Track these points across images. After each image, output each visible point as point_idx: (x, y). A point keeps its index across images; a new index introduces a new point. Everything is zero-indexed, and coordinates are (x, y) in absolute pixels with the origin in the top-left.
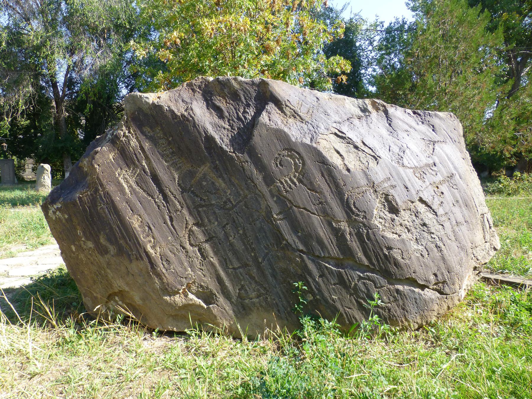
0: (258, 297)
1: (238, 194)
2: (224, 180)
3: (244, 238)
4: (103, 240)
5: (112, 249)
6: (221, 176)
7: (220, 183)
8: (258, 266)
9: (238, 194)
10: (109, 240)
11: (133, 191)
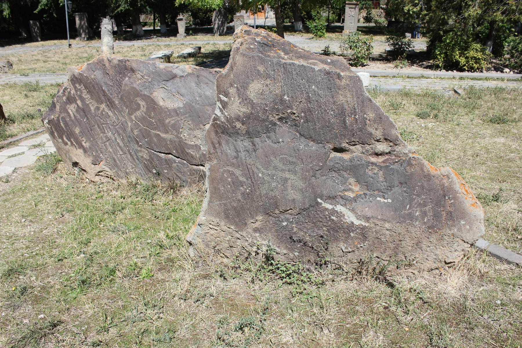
0: (132, 168)
3: (123, 140)
4: (65, 139)
5: (69, 143)
6: (110, 110)
7: (110, 113)
8: (130, 154)
10: (67, 139)
11: (74, 115)
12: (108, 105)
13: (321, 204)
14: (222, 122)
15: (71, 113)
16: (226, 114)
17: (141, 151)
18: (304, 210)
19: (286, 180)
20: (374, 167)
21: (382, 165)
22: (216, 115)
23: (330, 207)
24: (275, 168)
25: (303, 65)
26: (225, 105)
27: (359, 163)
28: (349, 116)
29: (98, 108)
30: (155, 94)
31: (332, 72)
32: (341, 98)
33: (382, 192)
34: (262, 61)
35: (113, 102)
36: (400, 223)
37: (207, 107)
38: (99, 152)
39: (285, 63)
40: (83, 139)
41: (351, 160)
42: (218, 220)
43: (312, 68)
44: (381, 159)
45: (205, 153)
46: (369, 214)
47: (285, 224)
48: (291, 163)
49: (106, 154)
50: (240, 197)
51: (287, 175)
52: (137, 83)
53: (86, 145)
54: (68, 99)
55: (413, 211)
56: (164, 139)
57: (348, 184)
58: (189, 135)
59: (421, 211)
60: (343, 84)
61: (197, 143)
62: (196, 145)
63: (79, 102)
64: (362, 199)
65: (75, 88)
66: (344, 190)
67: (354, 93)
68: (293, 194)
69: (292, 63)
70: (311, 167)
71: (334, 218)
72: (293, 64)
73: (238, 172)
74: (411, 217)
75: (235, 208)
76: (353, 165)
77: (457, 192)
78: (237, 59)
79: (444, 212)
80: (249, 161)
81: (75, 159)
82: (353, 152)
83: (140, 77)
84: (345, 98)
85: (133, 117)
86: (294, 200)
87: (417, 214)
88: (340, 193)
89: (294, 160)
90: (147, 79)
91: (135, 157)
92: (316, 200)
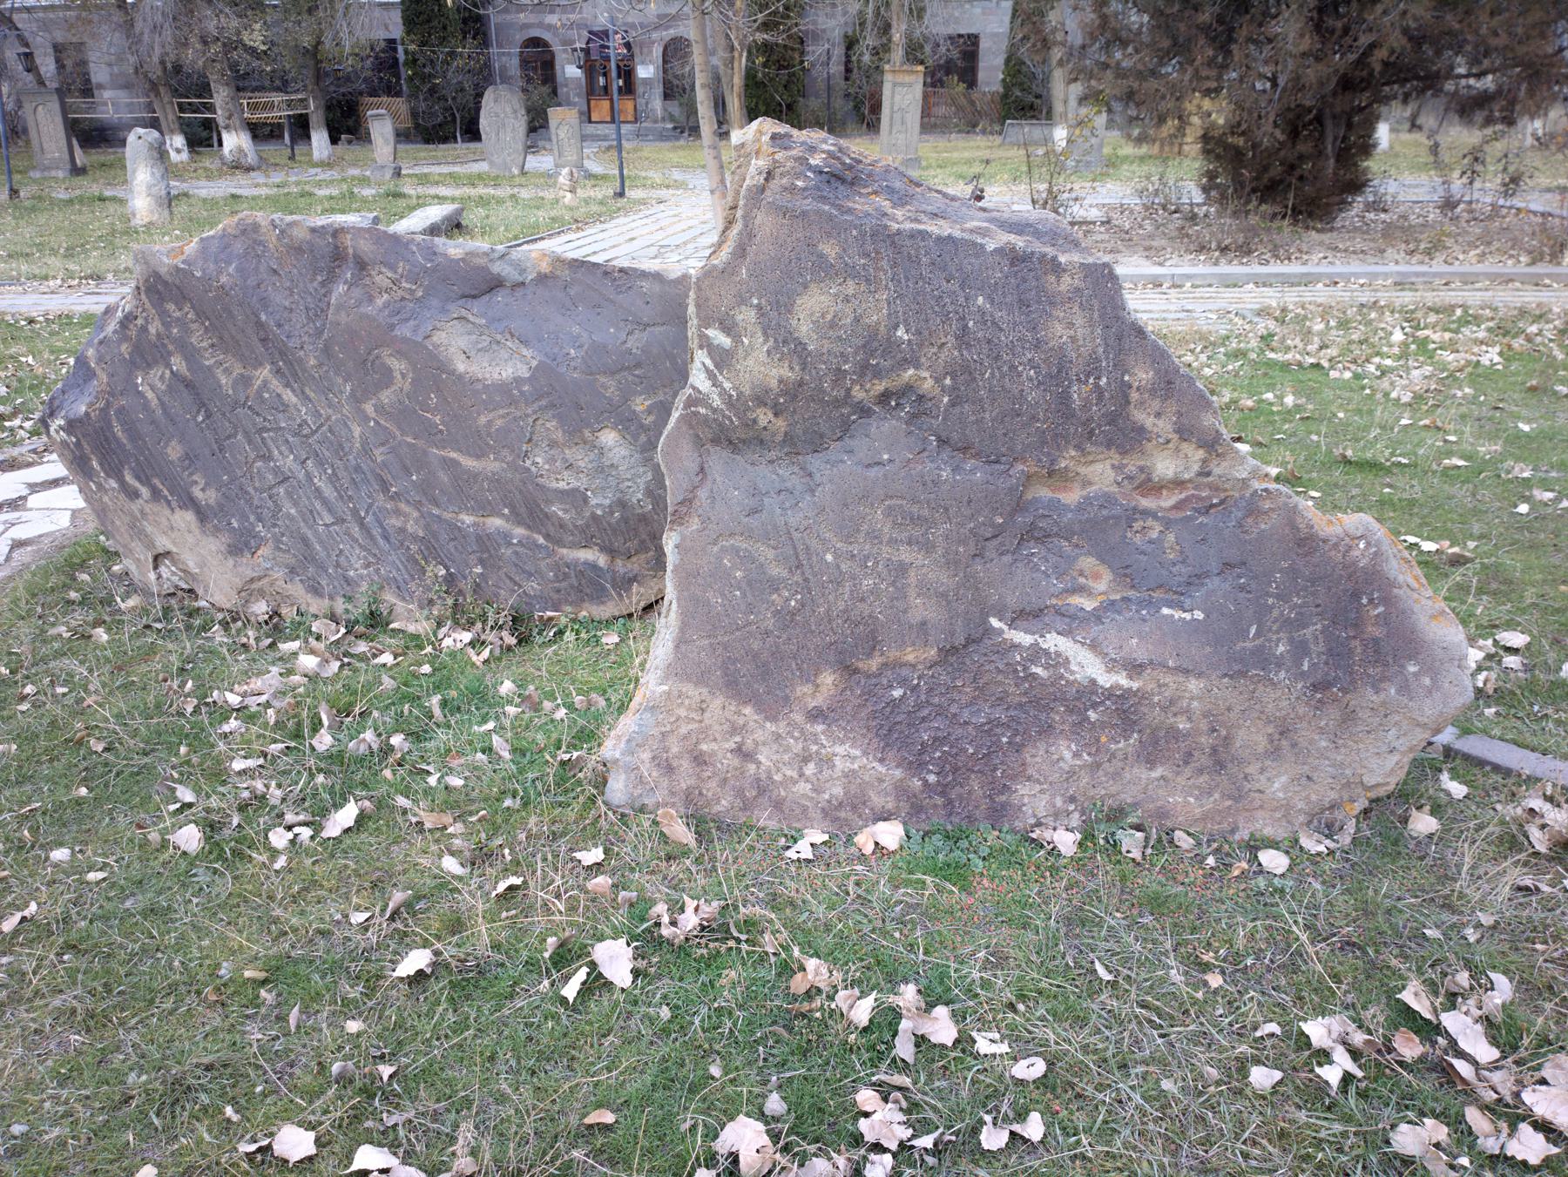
0: (367, 566)
1: (317, 414)
2: (293, 391)
3: (334, 479)
4: (129, 478)
5: (145, 492)
6: (287, 385)
7: (289, 396)
8: (362, 524)
9: (317, 414)
10: (138, 478)
11: (162, 404)
12: (278, 371)
13: (1001, 632)
14: (715, 410)
15: (150, 395)
16: (727, 385)
17: (398, 512)
18: (954, 650)
19: (903, 569)
20: (1150, 522)
21: (1174, 515)
22: (694, 388)
23: (1026, 639)
24: (874, 536)
25: (950, 237)
26: (722, 359)
27: (1105, 512)
28: (1079, 380)
29: (245, 381)
30: (439, 337)
31: (1033, 253)
32: (1059, 329)
33: (1176, 593)
34: (833, 228)
35: (300, 361)
36: (1231, 677)
37: (602, 379)
38: (252, 518)
39: (899, 232)
40: (195, 478)
41: (1080, 508)
42: (705, 691)
43: (974, 244)
44: (1168, 500)
45: (599, 512)
46: (1141, 656)
47: (897, 693)
48: (916, 520)
49: (275, 525)
50: (770, 623)
51: (906, 554)
52: (380, 302)
53: (206, 496)
54: (137, 349)
55: (1270, 641)
56: (474, 476)
57: (1075, 574)
58: (551, 461)
59: (1291, 641)
60: (1063, 288)
61: (575, 484)
62: (576, 490)
63: (178, 363)
64: (1119, 613)
65: (163, 314)
66: (1067, 591)
67: (1096, 315)
68: (920, 609)
69: (920, 232)
70: (971, 531)
71: (1039, 670)
72: (924, 235)
73: (766, 553)
74: (1262, 658)
75: (756, 656)
76: (1088, 520)
77: (1392, 584)
78: (757, 222)
79: (1357, 642)
80: (794, 519)
81: (163, 543)
82: (1087, 483)
83: (387, 283)
84: (1070, 330)
85: (369, 408)
86: (924, 623)
87: (1281, 649)
88: (1054, 601)
89: (925, 512)
90: (412, 292)
91: (376, 532)
92: (985, 622)
